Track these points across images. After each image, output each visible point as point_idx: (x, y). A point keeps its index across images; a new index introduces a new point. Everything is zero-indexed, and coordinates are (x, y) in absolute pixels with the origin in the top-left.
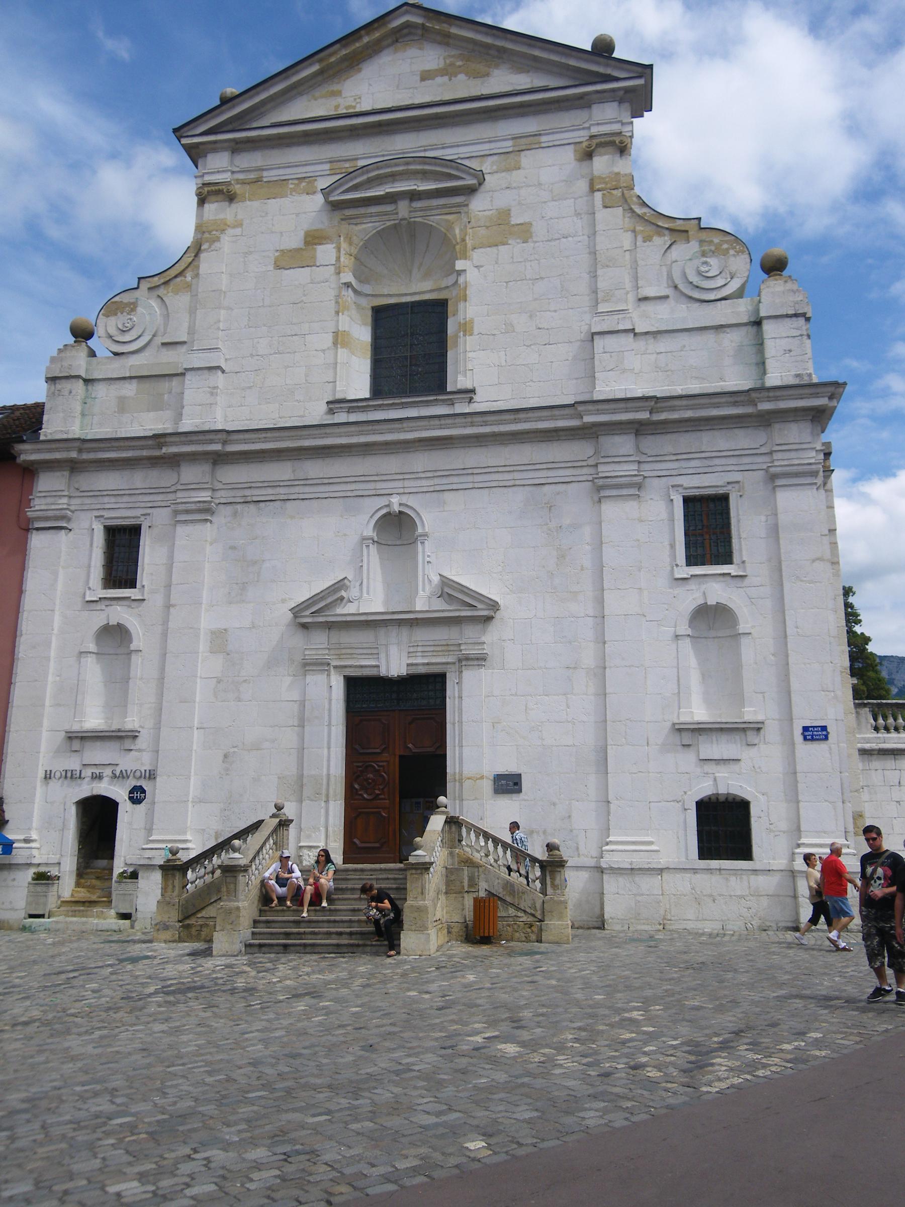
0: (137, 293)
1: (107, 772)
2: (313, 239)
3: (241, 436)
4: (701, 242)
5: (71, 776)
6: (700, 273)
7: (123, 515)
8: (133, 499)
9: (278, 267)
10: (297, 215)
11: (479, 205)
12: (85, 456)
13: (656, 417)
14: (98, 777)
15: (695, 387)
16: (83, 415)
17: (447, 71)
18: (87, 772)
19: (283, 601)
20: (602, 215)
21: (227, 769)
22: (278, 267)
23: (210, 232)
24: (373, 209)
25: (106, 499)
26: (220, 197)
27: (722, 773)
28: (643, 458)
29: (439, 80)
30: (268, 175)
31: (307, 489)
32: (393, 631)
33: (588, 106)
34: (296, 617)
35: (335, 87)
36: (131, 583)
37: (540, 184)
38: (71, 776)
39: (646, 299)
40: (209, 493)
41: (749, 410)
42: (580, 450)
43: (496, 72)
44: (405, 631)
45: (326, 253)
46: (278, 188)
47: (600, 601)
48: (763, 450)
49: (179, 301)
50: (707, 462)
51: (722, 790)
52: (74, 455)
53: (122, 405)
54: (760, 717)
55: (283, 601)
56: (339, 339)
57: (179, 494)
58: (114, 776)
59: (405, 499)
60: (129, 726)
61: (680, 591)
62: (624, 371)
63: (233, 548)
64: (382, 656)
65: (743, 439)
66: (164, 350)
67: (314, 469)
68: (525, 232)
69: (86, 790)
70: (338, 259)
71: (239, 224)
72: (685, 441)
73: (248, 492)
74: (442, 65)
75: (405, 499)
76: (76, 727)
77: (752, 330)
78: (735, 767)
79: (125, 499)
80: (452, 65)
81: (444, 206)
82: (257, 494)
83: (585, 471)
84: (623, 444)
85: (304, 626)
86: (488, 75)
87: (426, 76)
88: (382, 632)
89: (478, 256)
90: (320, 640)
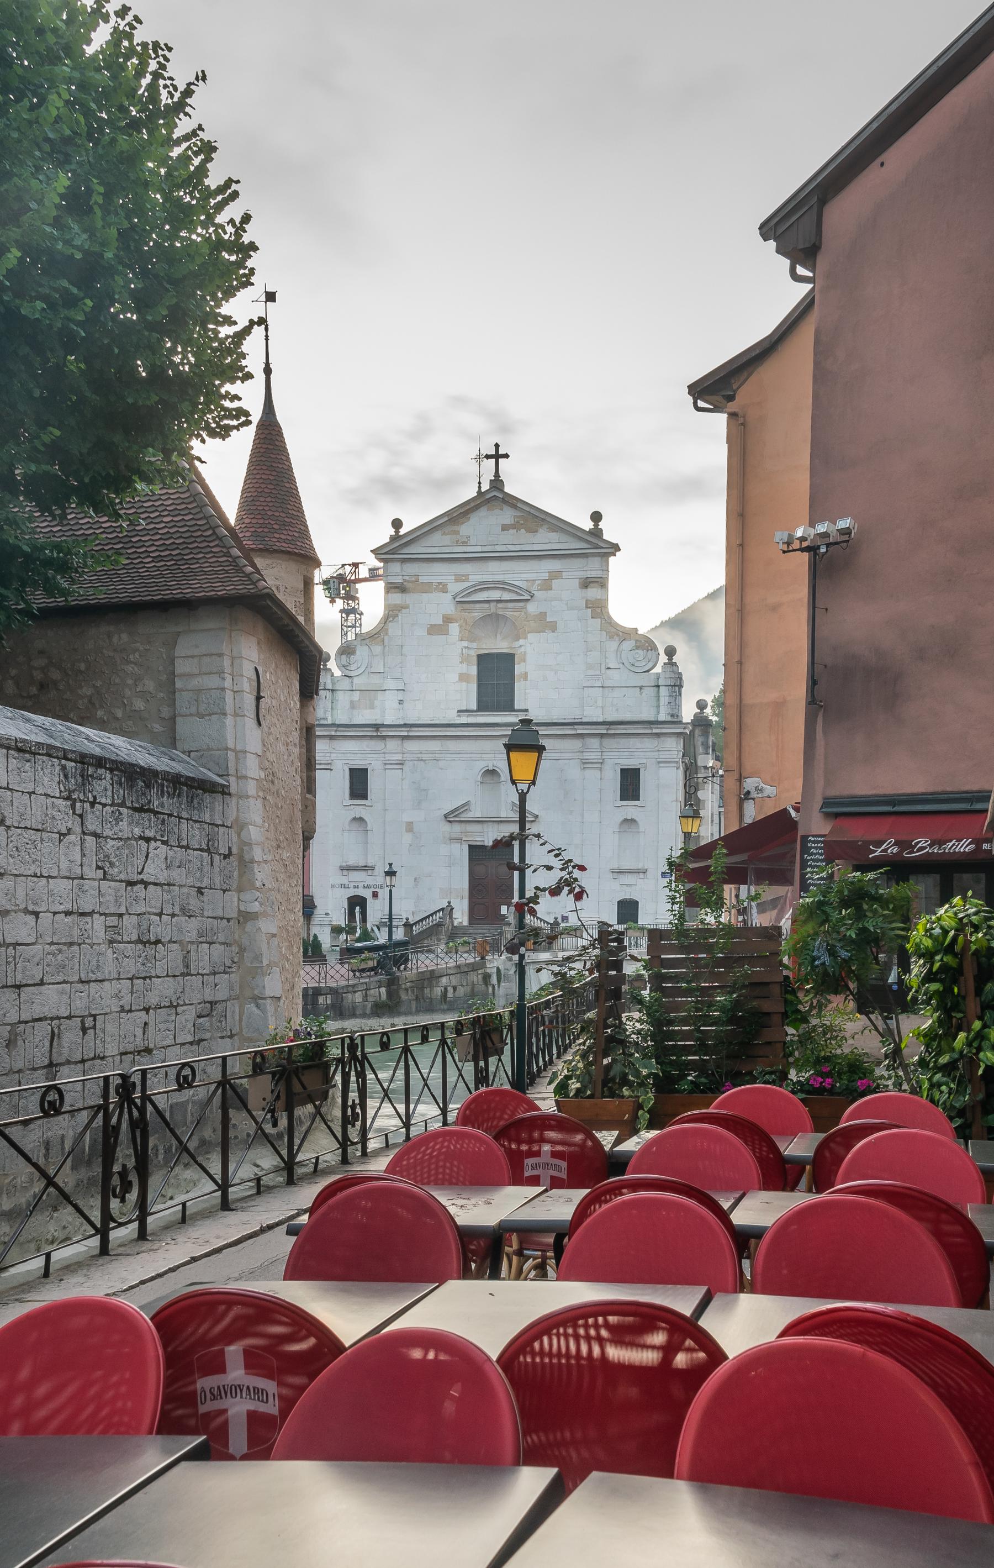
0: (355, 643)
1: (361, 885)
2: (448, 620)
3: (416, 729)
4: (637, 641)
5: (344, 886)
6: (634, 658)
7: (358, 763)
8: (363, 755)
9: (429, 633)
10: (438, 604)
11: (532, 608)
12: (338, 733)
13: (610, 732)
14: (358, 887)
15: (628, 717)
16: (332, 708)
17: (515, 526)
18: (352, 885)
19: (439, 809)
20: (591, 621)
21: (416, 885)
22: (429, 633)
23: (392, 611)
24: (478, 606)
25: (349, 755)
26: (397, 590)
27: (628, 889)
28: (604, 750)
29: (511, 531)
30: (422, 579)
31: (449, 755)
32: (491, 825)
33: (587, 557)
34: (446, 818)
35: (456, 528)
36: (364, 797)
37: (561, 600)
38: (344, 886)
39: (609, 668)
40: (401, 755)
41: (649, 731)
42: (577, 743)
43: (541, 530)
44: (496, 825)
45: (454, 628)
46: (427, 588)
47: (582, 815)
48: (656, 749)
49: (377, 649)
50: (632, 753)
51: (628, 897)
52: (333, 733)
53: (353, 705)
54: (646, 868)
55: (439, 809)
56: (463, 678)
57: (386, 755)
58: (364, 887)
59: (495, 762)
60: (370, 865)
61: (618, 810)
62: (597, 707)
63: (414, 782)
64: (486, 836)
65: (649, 743)
66: (372, 675)
67: (451, 745)
68: (553, 627)
69: (352, 892)
70: (460, 632)
71: (407, 607)
72: (623, 742)
73: (419, 755)
74: (513, 522)
75: (495, 762)
76: (344, 864)
77: (656, 689)
78: (633, 887)
79: (359, 755)
80: (518, 522)
81: (514, 608)
82: (425, 757)
83: (578, 754)
84: (595, 742)
85: (450, 821)
86: (536, 531)
87: (505, 528)
88: (485, 825)
89: (529, 635)
90: (457, 828)
